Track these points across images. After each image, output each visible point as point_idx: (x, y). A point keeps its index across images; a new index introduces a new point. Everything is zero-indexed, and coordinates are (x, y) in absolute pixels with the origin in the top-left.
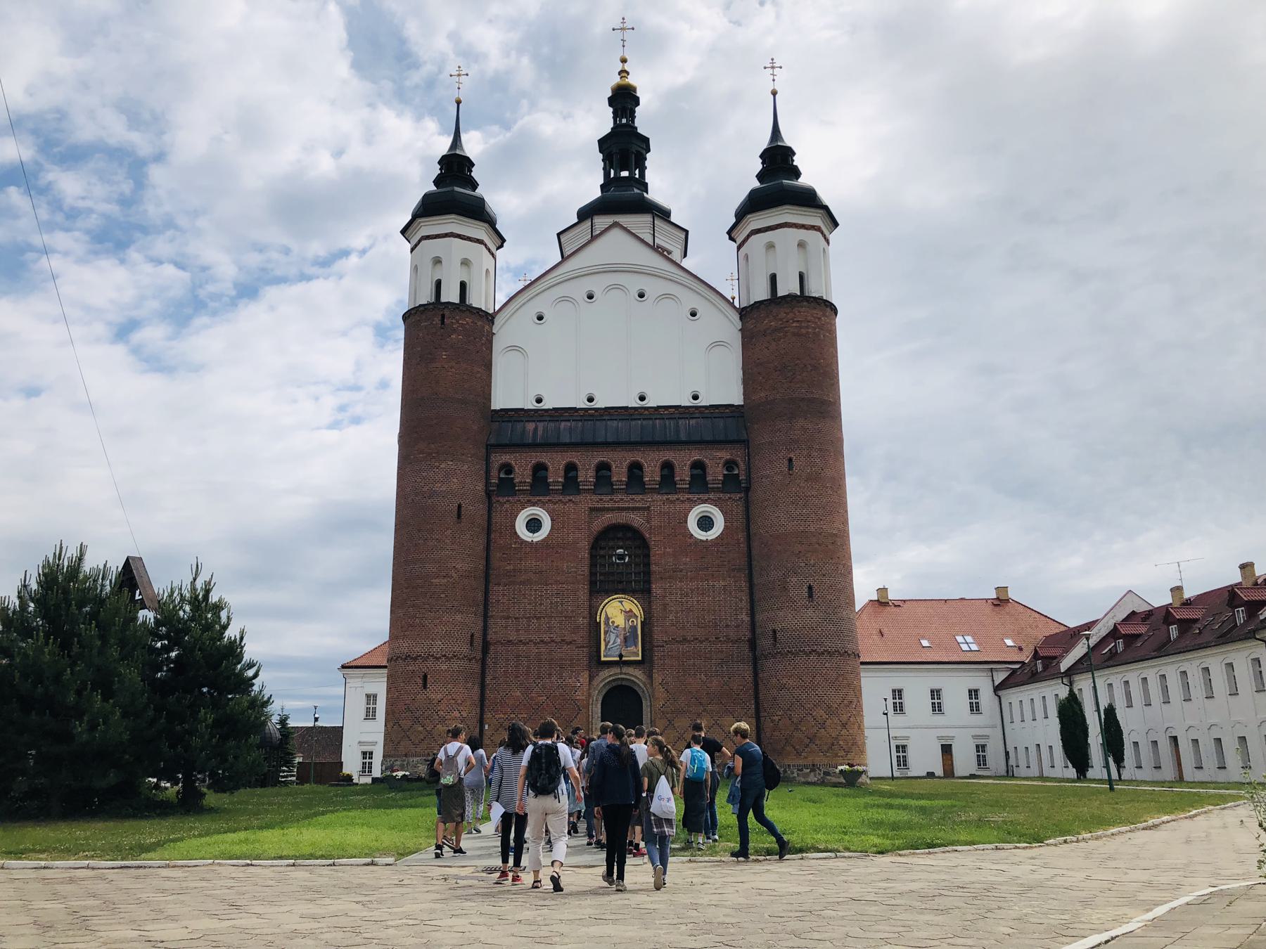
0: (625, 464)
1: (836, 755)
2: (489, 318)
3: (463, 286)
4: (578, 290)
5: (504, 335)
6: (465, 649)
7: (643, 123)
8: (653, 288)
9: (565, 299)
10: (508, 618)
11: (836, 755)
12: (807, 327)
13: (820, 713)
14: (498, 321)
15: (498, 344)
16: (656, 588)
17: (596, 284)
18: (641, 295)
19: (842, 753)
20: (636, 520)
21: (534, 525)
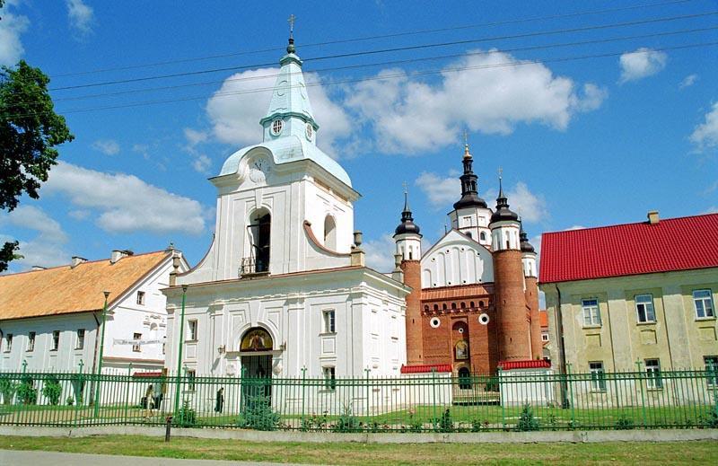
2: (419, 262)
3: (410, 254)
4: (443, 250)
5: (424, 265)
6: (418, 359)
7: (475, 170)
16: (471, 340)
20: (464, 320)
21: (436, 323)
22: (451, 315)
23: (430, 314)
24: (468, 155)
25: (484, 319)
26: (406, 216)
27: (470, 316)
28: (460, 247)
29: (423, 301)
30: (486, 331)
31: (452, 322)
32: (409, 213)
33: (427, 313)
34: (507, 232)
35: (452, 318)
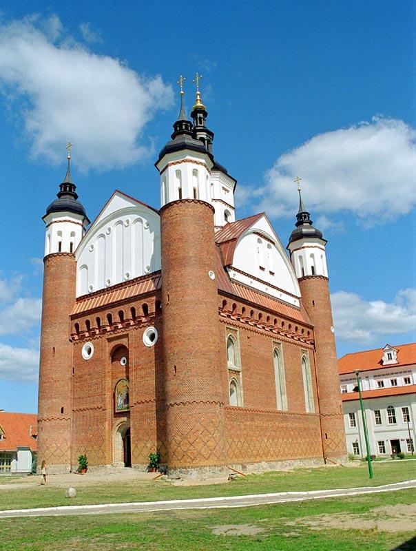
0: (117, 313)
1: (186, 461)
4: (103, 230)
6: (59, 415)
8: (132, 217)
9: (102, 236)
10: (80, 398)
11: (186, 461)
12: (176, 218)
13: (178, 438)
14: (77, 256)
15: (78, 266)
17: (111, 224)
18: (128, 222)
19: (189, 460)
20: (124, 341)
22: (107, 336)
23: (82, 338)
24: (199, 104)
25: (152, 337)
26: (68, 189)
27: (132, 332)
28: (123, 218)
29: (73, 317)
30: (153, 358)
31: (109, 347)
32: (72, 186)
33: (79, 336)
34: (179, 173)
35: (110, 340)
